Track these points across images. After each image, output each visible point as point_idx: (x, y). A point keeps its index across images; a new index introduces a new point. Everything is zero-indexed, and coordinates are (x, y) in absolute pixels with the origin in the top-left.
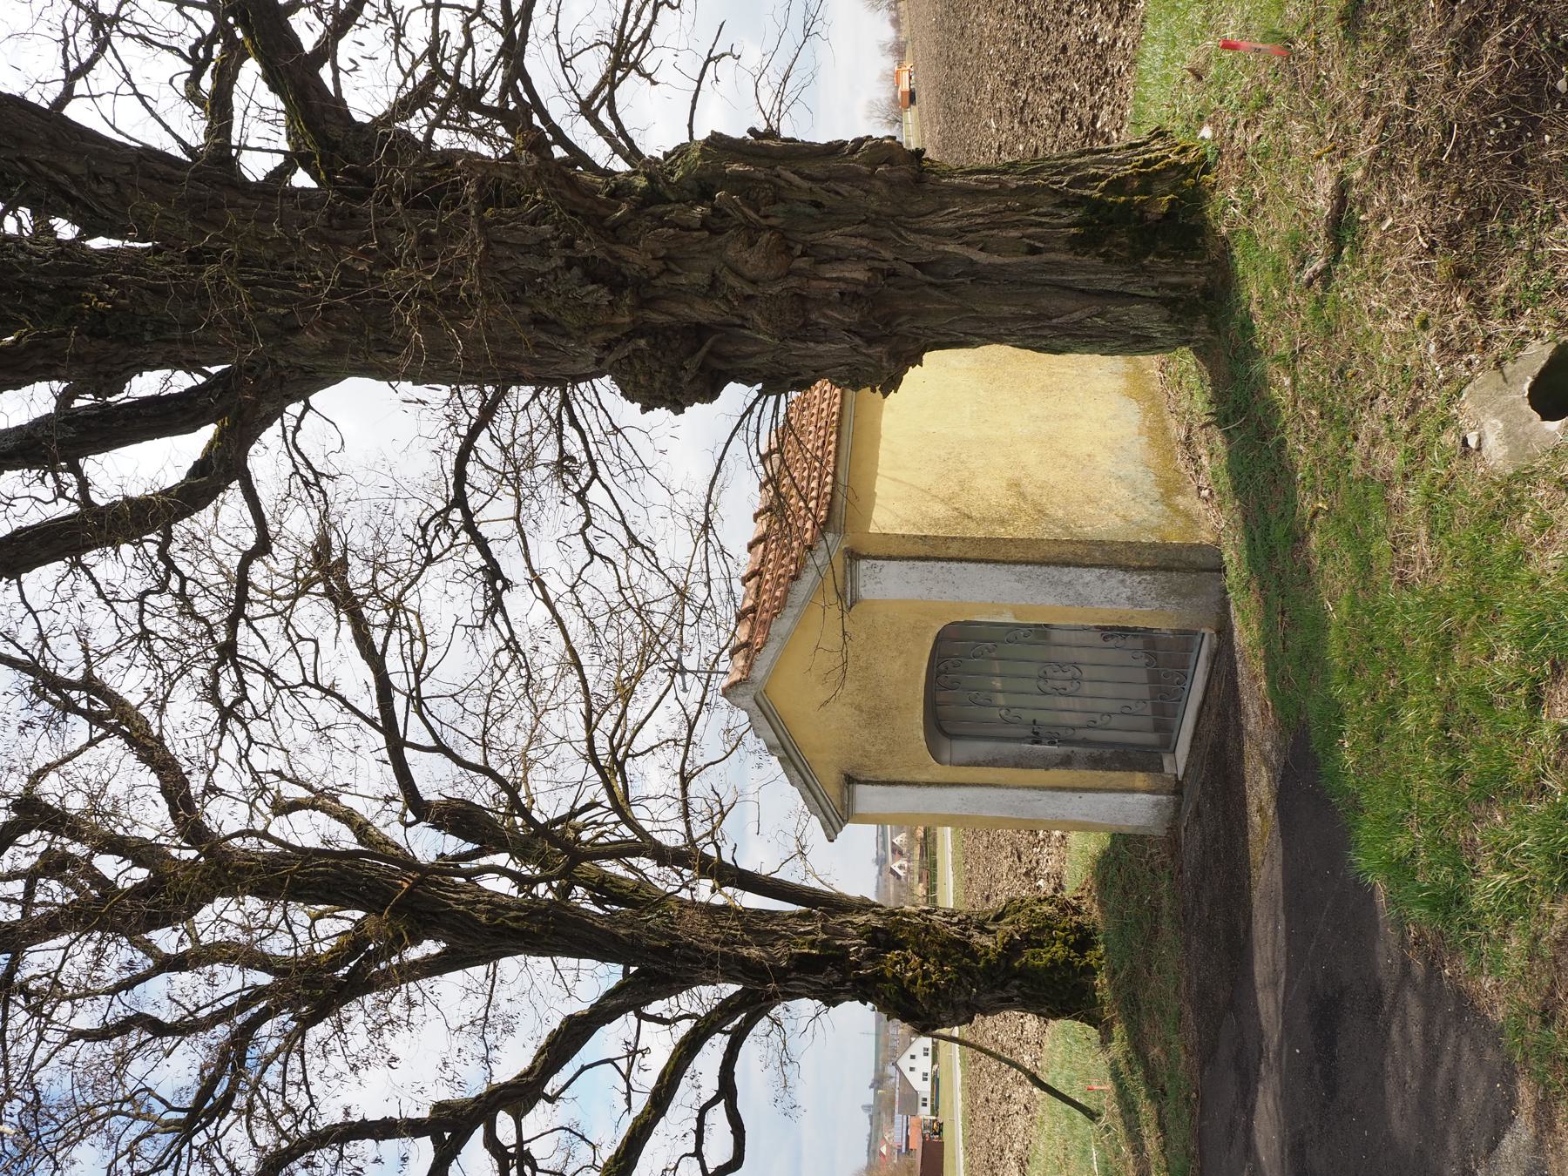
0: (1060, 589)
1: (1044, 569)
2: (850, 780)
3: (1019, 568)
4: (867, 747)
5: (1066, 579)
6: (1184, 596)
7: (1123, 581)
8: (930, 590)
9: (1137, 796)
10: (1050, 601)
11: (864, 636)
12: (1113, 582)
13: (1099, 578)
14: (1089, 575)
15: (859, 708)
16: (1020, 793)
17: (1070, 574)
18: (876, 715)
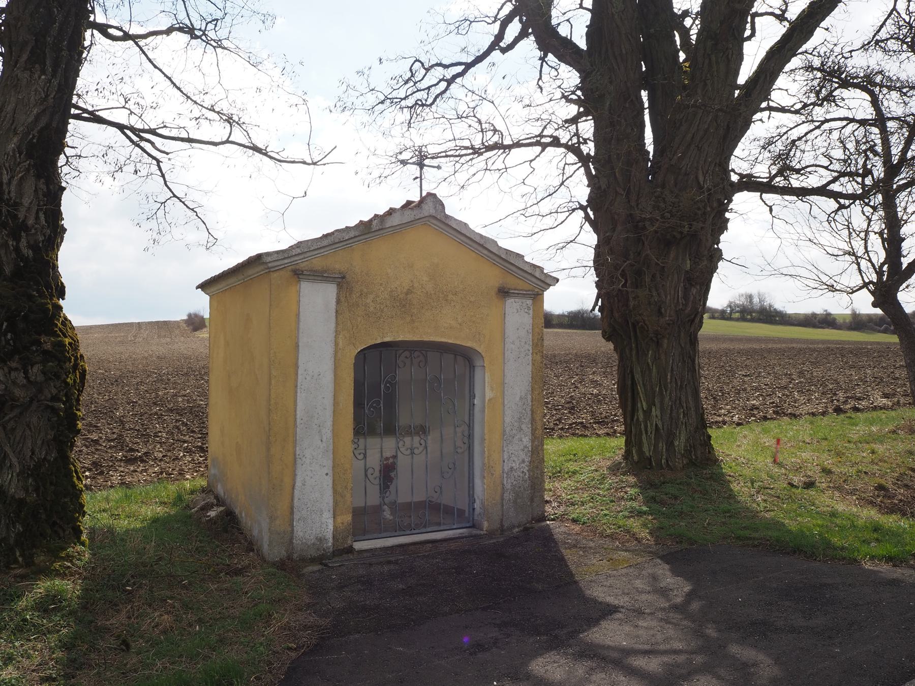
0: (516, 424)
1: (529, 413)
2: (342, 281)
3: (529, 397)
4: (371, 297)
5: (523, 427)
6: (515, 502)
7: (523, 461)
8: (513, 343)
9: (331, 521)
10: (508, 420)
11: (472, 299)
12: (522, 455)
13: (526, 447)
14: (527, 441)
15: (409, 292)
16: (329, 423)
17: (527, 428)
18: (404, 304)
